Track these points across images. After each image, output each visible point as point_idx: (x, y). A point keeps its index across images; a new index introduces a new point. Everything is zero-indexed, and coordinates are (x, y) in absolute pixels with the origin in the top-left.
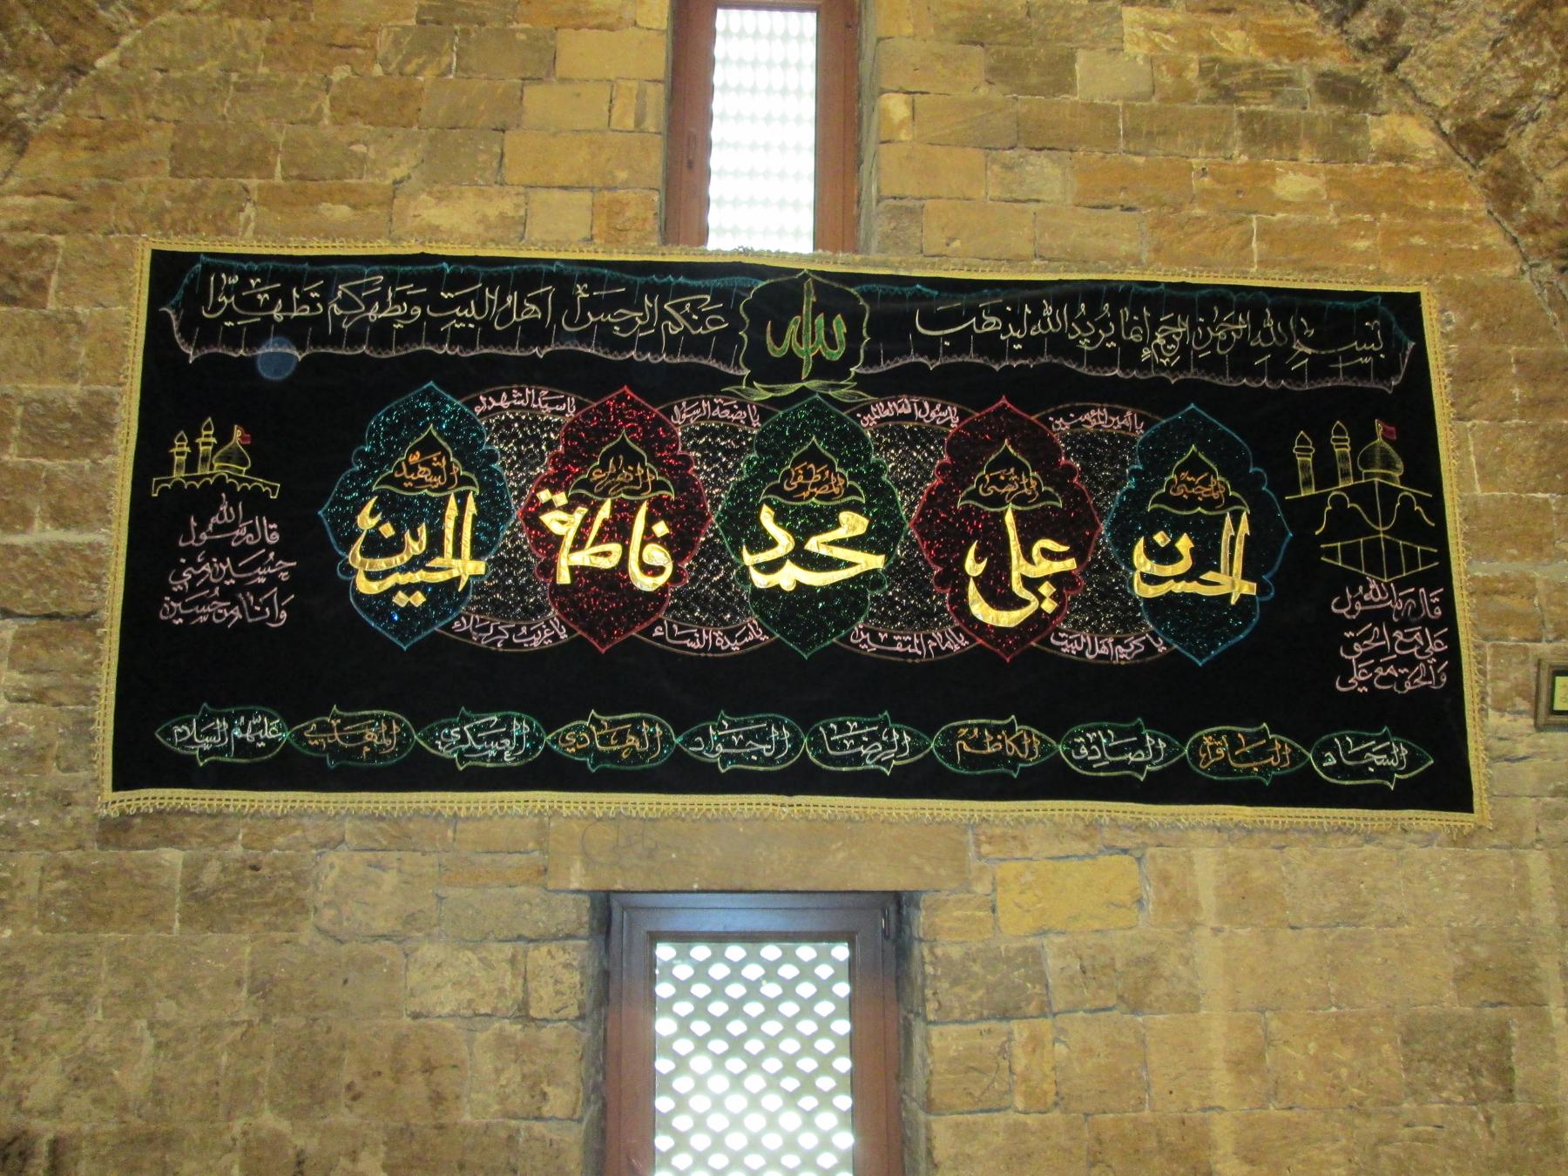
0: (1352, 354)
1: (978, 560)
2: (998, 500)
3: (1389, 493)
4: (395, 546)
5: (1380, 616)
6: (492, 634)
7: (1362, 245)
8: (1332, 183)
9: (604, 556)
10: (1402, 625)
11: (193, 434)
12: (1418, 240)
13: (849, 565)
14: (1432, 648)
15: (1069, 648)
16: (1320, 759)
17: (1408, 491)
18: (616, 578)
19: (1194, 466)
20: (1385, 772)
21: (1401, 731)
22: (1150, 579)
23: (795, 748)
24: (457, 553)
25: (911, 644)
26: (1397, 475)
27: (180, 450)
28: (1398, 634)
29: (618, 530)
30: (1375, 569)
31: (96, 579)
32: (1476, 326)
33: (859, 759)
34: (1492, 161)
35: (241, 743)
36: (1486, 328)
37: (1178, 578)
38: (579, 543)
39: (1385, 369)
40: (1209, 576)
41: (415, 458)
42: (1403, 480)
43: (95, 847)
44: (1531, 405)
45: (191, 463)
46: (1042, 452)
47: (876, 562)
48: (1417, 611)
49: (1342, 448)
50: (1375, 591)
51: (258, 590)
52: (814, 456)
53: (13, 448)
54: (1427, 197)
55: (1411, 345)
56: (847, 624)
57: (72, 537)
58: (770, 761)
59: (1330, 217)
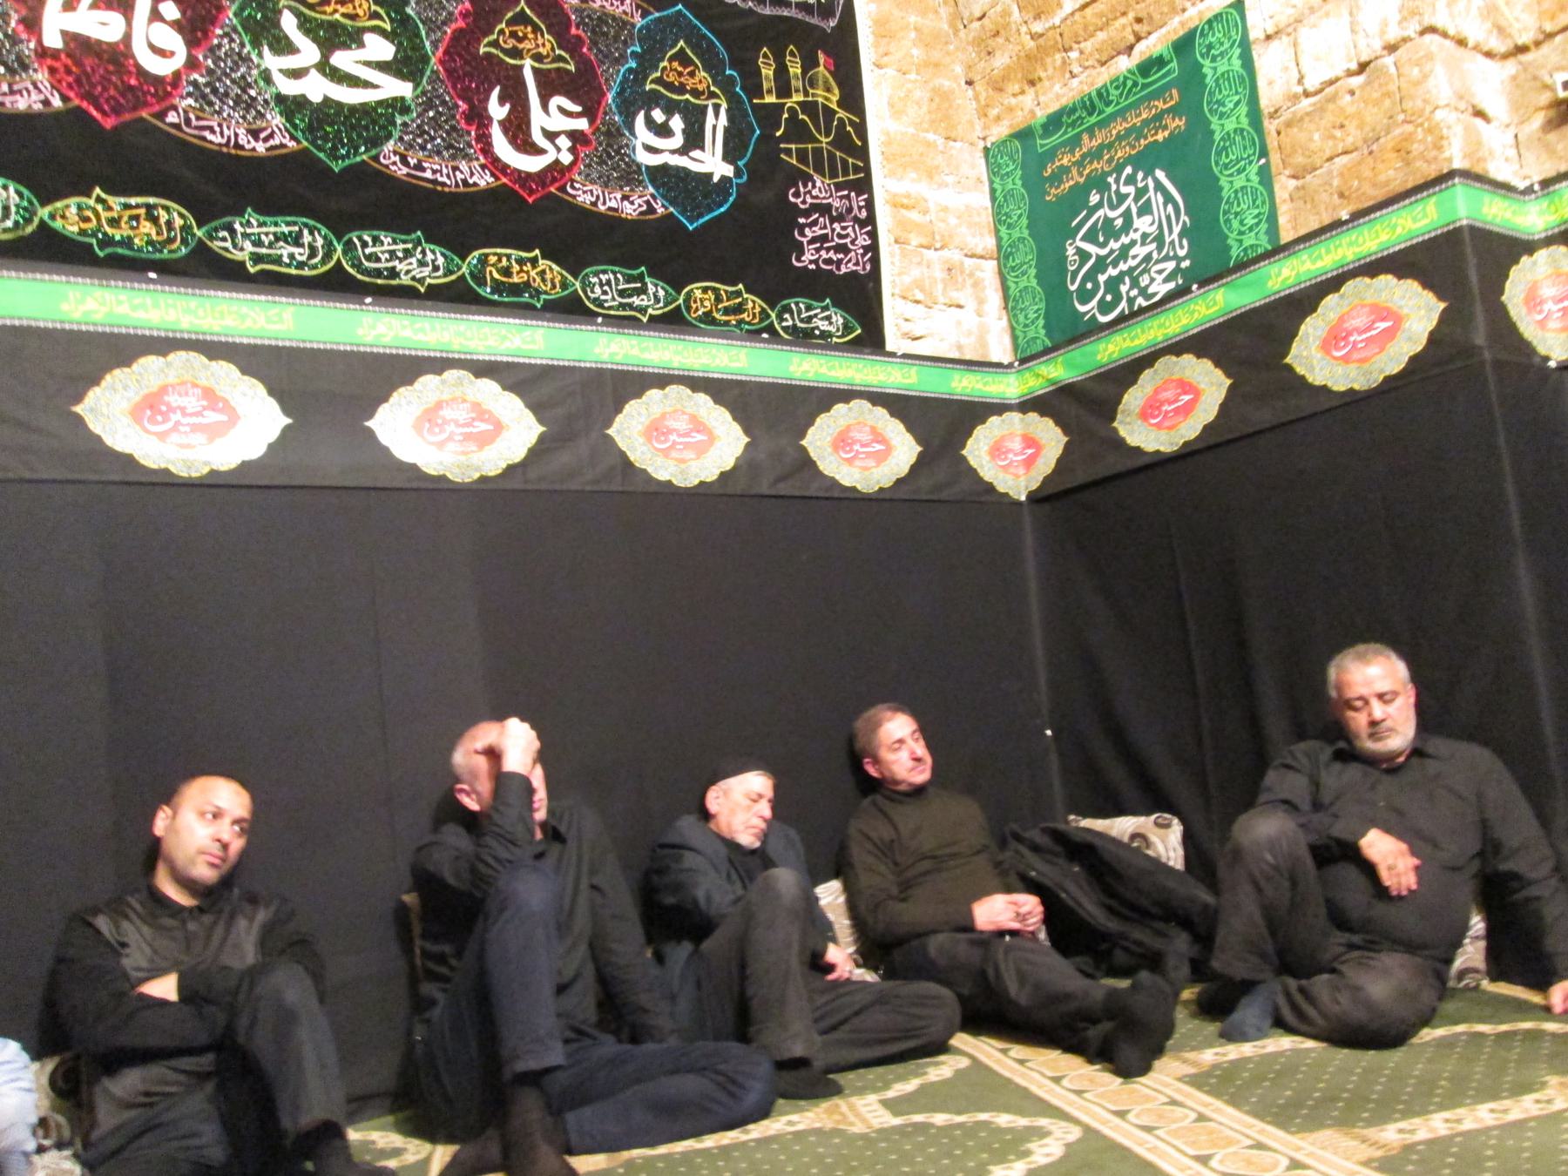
1: (502, 101)
2: (516, 53)
3: (829, 113)
5: (825, 209)
10: (840, 218)
15: (584, 199)
16: (781, 319)
17: (841, 114)
18: (117, 56)
19: (681, 57)
23: (328, 256)
25: (441, 172)
26: (835, 98)
28: (836, 225)
30: (821, 172)
33: (393, 273)
37: (673, 152)
40: (696, 154)
42: (839, 104)
47: (404, 89)
49: (795, 69)
50: (820, 189)
56: (375, 142)
58: (301, 265)
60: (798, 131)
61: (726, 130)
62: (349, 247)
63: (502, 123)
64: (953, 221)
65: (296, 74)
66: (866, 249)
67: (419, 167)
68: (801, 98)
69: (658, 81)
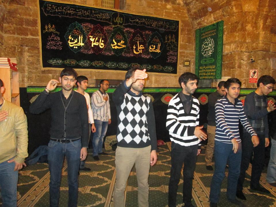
0: (172, 27)
1: (135, 47)
2: (137, 40)
3: (174, 42)
4: (73, 41)
5: (171, 55)
6: (86, 52)
7: (174, 15)
8: (173, 7)
9: (96, 44)
10: (173, 56)
11: (48, 26)
12: (180, 15)
13: (122, 46)
14: (175, 58)
15: (143, 57)
17: (175, 42)
19: (156, 38)
20: (170, 70)
21: (172, 66)
22: (151, 50)
23: (116, 65)
24: (81, 42)
25: (128, 55)
26: (175, 40)
27: (46, 27)
29: (98, 41)
30: (171, 50)
31: (38, 43)
32: (184, 25)
33: (122, 67)
34: (188, 7)
35: (57, 63)
36: (185, 25)
37: (153, 50)
38: (94, 42)
39: (175, 29)
40: (156, 50)
41: (75, 31)
43: (41, 74)
44: (187, 34)
45: (48, 29)
46: (142, 35)
48: (174, 55)
49: (170, 37)
50: (171, 52)
51: (58, 45)
52: (119, 34)
53: (24, 25)
54: (181, 10)
55: (177, 27)
56: (122, 53)
57: (34, 37)
58: (114, 67)
59: (172, 11)
60: (169, 45)
61: (160, 46)
62: (118, 65)
63: (135, 49)
64: (188, 54)
65: (114, 46)
66: (176, 59)
67: (126, 55)
68: (170, 41)
69: (153, 41)
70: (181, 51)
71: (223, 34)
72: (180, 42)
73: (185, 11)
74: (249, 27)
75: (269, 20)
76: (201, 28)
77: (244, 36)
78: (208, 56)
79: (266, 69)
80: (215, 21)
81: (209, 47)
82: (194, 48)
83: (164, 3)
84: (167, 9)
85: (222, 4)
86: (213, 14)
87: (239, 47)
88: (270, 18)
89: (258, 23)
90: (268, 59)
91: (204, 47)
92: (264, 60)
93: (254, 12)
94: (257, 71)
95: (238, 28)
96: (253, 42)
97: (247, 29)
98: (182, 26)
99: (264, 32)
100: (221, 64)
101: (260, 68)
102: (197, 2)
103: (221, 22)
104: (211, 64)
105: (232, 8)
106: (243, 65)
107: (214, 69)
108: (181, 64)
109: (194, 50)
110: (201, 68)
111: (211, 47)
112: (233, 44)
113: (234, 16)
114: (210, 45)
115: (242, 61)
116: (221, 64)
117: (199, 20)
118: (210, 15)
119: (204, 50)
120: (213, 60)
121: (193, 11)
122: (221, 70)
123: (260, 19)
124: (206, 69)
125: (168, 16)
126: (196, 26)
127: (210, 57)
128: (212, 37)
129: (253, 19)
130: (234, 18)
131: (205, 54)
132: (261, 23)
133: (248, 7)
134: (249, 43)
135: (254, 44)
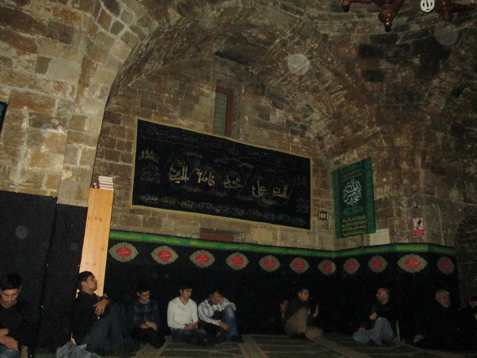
4: (175, 173)
6: (190, 189)
7: (304, 150)
8: (301, 141)
11: (145, 151)
13: (237, 186)
18: (206, 184)
20: (301, 223)
24: (184, 176)
27: (143, 153)
31: (130, 172)
35: (152, 200)
41: (178, 160)
43: (129, 213)
44: (321, 177)
45: (145, 155)
47: (242, 186)
50: (302, 199)
51: (155, 177)
53: (116, 148)
57: (126, 164)
59: (300, 146)
63: (254, 191)
65: (227, 185)
70: (315, 198)
71: (372, 173)
72: (313, 186)
73: (317, 147)
74: (404, 165)
75: (428, 157)
76: (340, 168)
77: (399, 177)
78: (354, 203)
79: (433, 217)
80: (360, 157)
81: (355, 192)
82: (331, 196)
83: (290, 135)
84: (294, 143)
85: (367, 137)
86: (356, 150)
87: (394, 189)
88: (430, 155)
89: (415, 159)
90: (433, 205)
91: (346, 192)
92: (429, 206)
93: (408, 147)
94: (422, 219)
95: (391, 166)
96: (412, 182)
97: (402, 167)
98: (314, 165)
99: (424, 171)
100: (374, 213)
101: (426, 216)
102: (333, 136)
103: (367, 159)
104: (360, 214)
105: (381, 142)
106: (403, 213)
107: (364, 220)
108: (315, 216)
109: (331, 197)
110: (344, 221)
111: (357, 192)
112: (387, 186)
113: (384, 150)
114: (355, 189)
115: (401, 207)
116: (374, 213)
117: (338, 158)
118: (352, 151)
119: (347, 196)
120: (362, 209)
121: (328, 147)
122: (375, 220)
123: (417, 155)
124: (353, 221)
125: (295, 152)
126: (333, 167)
127: (357, 205)
128: (356, 179)
129: (407, 154)
130: (385, 154)
131: (348, 201)
132: (419, 160)
133: (400, 141)
134: (407, 184)
135: (414, 186)
